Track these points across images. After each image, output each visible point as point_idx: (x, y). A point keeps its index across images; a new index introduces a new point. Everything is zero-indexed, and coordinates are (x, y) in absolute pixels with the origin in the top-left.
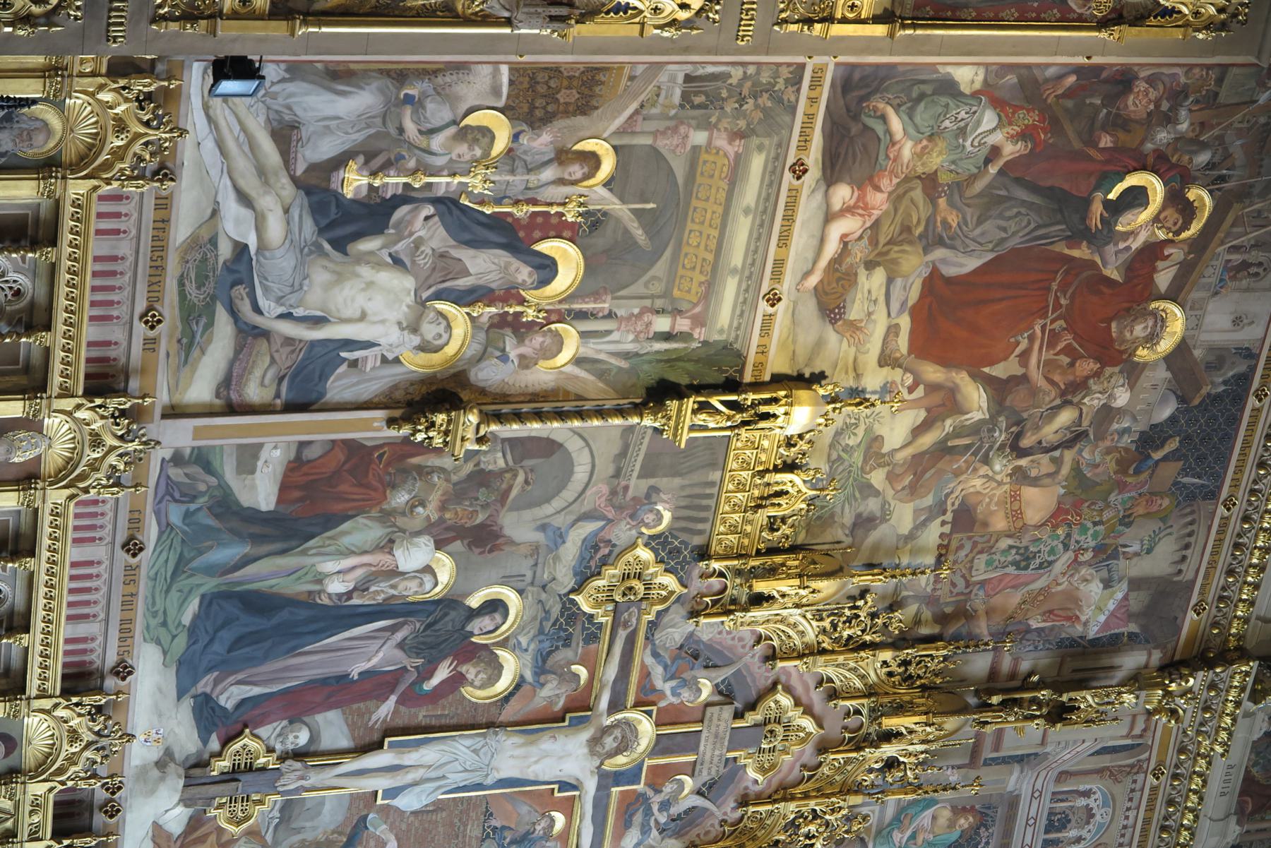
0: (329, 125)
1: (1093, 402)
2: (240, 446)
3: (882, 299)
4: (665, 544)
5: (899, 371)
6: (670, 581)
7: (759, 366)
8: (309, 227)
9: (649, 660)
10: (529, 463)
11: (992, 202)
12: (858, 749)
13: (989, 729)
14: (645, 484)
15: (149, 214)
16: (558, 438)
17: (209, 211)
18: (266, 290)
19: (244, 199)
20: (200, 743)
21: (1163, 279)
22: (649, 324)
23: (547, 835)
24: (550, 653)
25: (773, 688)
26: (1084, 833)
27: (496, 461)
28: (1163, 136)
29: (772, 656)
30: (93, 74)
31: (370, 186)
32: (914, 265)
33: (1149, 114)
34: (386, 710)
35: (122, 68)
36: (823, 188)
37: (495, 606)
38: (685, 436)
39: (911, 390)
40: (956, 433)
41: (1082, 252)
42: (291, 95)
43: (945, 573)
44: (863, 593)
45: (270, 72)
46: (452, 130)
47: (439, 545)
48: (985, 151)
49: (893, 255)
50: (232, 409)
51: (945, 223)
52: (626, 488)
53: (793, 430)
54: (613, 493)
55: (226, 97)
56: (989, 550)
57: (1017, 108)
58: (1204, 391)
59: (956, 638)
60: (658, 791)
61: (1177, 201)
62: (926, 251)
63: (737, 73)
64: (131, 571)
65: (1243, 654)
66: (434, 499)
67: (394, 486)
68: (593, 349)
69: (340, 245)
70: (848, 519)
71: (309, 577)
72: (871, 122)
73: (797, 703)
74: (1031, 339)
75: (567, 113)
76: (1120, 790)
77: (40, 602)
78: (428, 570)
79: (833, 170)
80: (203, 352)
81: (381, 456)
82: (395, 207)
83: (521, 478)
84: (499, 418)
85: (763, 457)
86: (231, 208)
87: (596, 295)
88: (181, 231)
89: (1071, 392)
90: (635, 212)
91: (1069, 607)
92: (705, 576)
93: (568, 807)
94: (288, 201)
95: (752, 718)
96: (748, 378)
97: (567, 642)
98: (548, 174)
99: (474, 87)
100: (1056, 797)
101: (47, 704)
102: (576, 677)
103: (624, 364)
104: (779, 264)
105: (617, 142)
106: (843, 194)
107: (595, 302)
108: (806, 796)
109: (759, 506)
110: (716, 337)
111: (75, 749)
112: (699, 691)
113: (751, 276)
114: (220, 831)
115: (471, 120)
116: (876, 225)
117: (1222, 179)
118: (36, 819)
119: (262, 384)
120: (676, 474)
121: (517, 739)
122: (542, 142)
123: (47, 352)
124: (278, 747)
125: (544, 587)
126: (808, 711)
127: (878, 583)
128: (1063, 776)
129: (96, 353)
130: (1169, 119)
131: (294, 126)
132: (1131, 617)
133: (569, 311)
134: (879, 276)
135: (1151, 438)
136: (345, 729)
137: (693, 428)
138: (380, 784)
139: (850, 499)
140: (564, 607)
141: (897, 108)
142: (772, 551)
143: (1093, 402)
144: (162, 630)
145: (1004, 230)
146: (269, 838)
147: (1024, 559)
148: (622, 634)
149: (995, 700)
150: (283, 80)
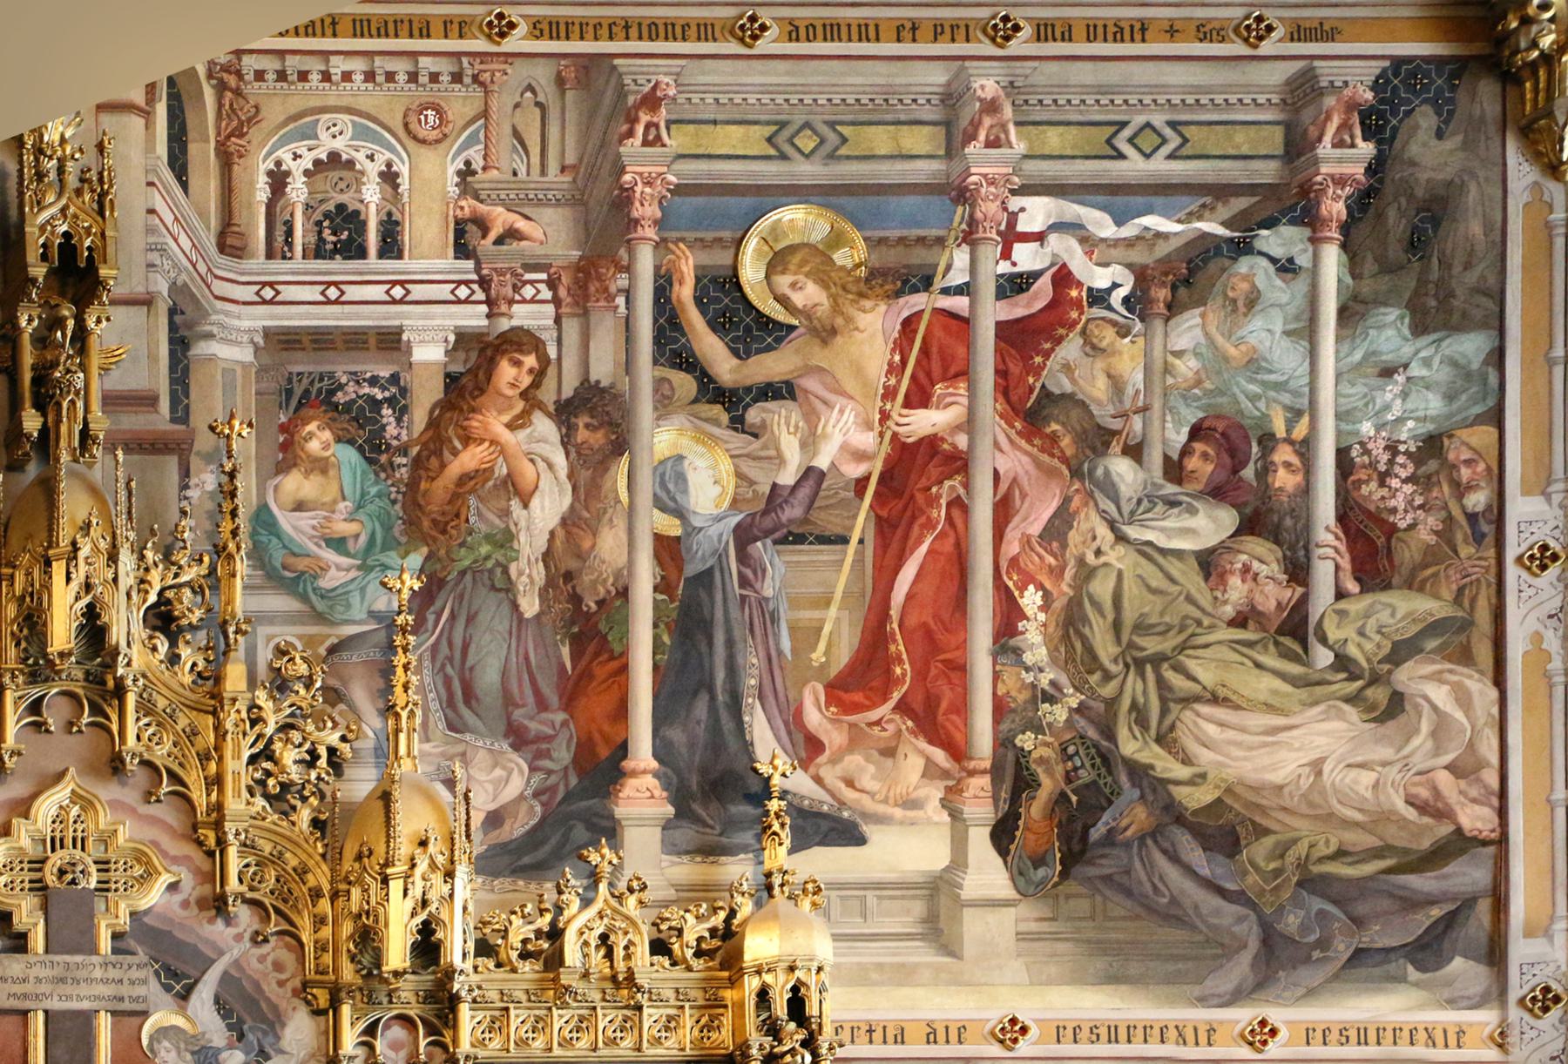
13: (100, 423)
26: (373, 170)
128: (230, 242)
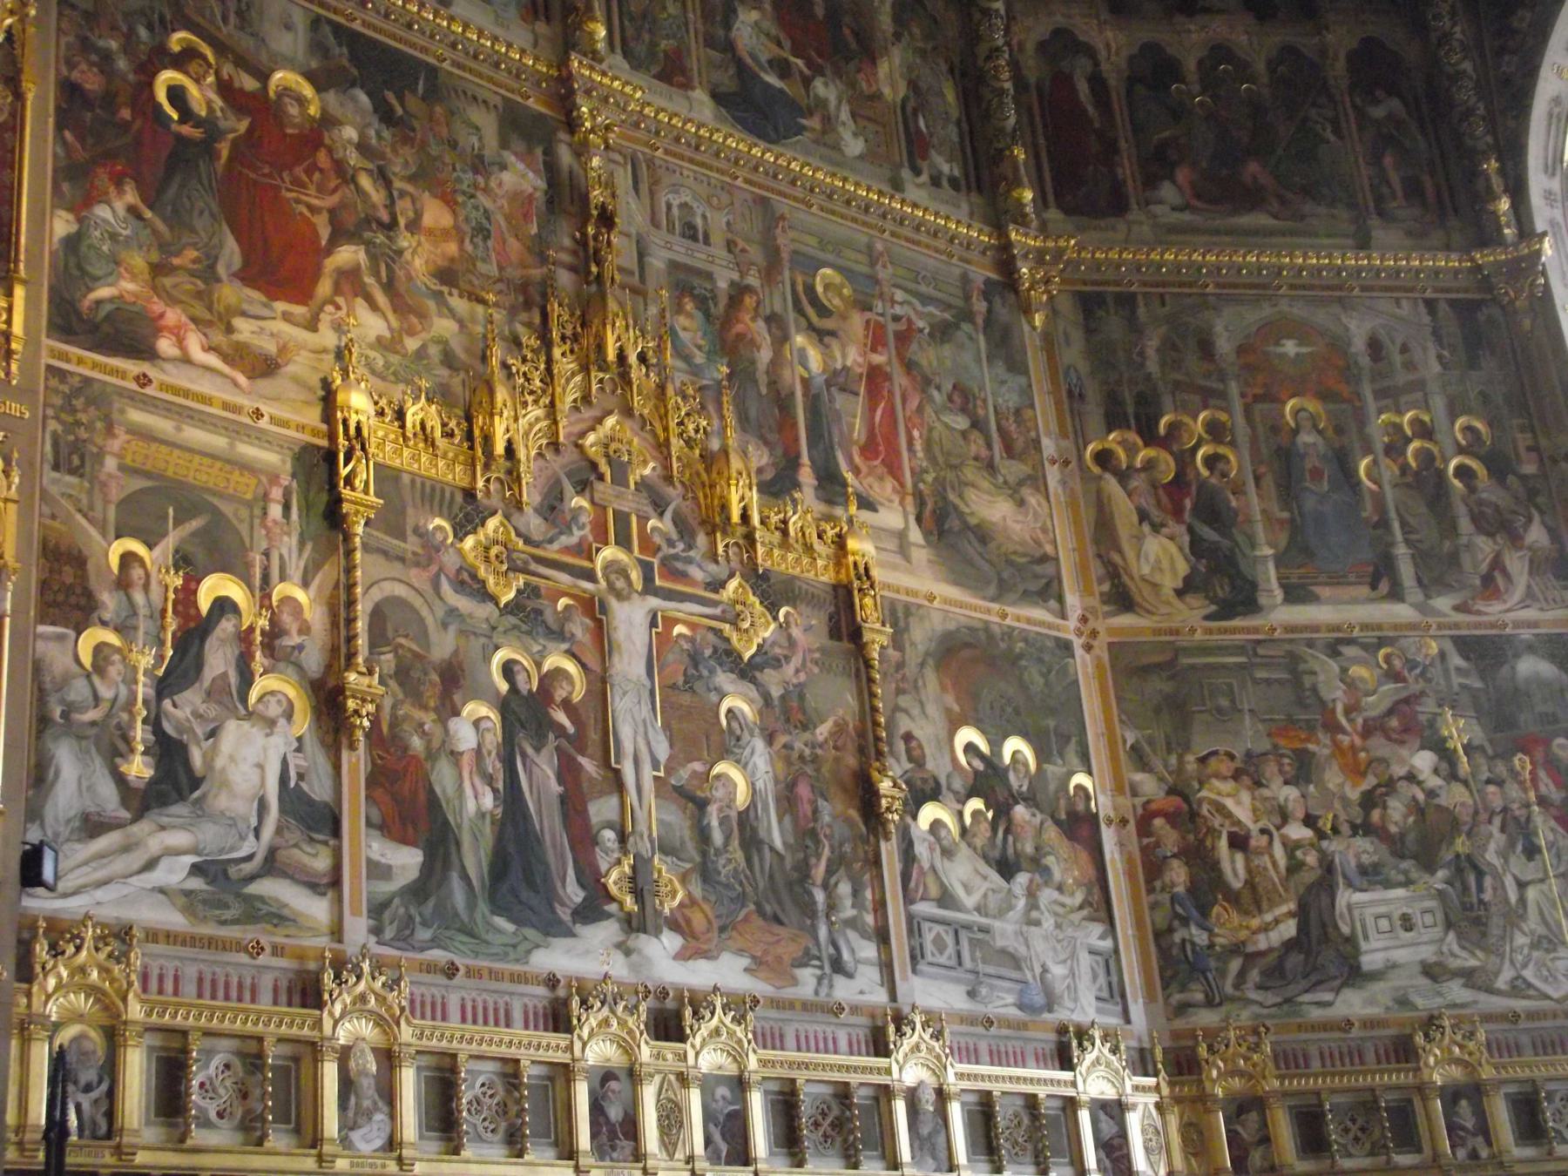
0: (85, 787)
1: (353, 158)
2: (368, 877)
3: (261, 323)
4: (462, 526)
5: (322, 316)
6: (492, 523)
7: (315, 432)
8: (179, 809)
9: (556, 546)
10: (390, 634)
11: (178, 219)
12: (629, 383)
13: (617, 277)
14: (412, 538)
15: (160, 948)
16: (369, 609)
17: (161, 896)
18: (232, 849)
19: (150, 865)
20: (612, 920)
21: (249, 83)
22: (275, 522)
23: (691, 640)
24: (548, 628)
25: (577, 446)
27: (388, 660)
28: (122, 64)
29: (555, 445)
30: (29, 995)
31: (144, 753)
32: (230, 292)
33: (102, 72)
34: (589, 765)
35: (25, 972)
36: (161, 363)
37: (508, 669)
38: (372, 498)
39: (338, 308)
40: (377, 275)
41: (224, 149)
42: (56, 819)
43: (491, 297)
44: (505, 366)
45: (34, 836)
46: (96, 679)
47: (457, 713)
48: (131, 219)
49: (222, 309)
50: (336, 882)
51: (194, 261)
52: (414, 554)
53: (371, 410)
54: (417, 564)
55: (57, 877)
56: (472, 260)
57: (92, 186)
58: (345, 62)
59: (544, 296)
60: (659, 549)
61: (181, 61)
62: (218, 280)
63: (53, 425)
64: (469, 973)
65: (564, 63)
66: (418, 714)
67: (406, 748)
68: (296, 572)
69: (196, 783)
70: (445, 372)
71: (480, 823)
72: (102, 313)
73: (593, 429)
74: (298, 201)
75: (84, 577)
76: (667, 180)
77: (494, 1050)
78: (476, 723)
79: (145, 352)
80: (286, 906)
81: (381, 757)
82: (164, 733)
83: (402, 641)
84: (351, 656)
85: (392, 436)
86: (159, 876)
87: (249, 566)
88: (174, 919)
89: (345, 175)
90: (176, 525)
91: (521, 201)
92: (488, 492)
93: (670, 622)
94: (153, 827)
95: (604, 468)
96: (324, 443)
97: (539, 612)
98: (139, 597)
99: (57, 658)
100: (671, 229)
101: (577, 1046)
102: (567, 607)
103: (309, 546)
104: (226, 406)
105: (112, 534)
106: (165, 345)
107: (253, 566)
108: (666, 429)
109: (433, 445)
110: (288, 466)
111: (614, 1022)
112: (581, 508)
113: (237, 431)
114: (681, 905)
115: (87, 660)
116: (194, 320)
117: (162, 20)
118: (670, 1056)
119: (315, 856)
120: (403, 512)
121: (616, 659)
122: (109, 601)
123: (281, 1040)
124: (616, 855)
125: (494, 628)
126: (600, 420)
127: (497, 353)
128: (655, 223)
129: (283, 998)
130: (107, 57)
131: (86, 818)
132: (530, 151)
133: (262, 589)
134: (238, 322)
135: (386, 115)
136: (602, 800)
137: (366, 491)
138: (648, 773)
139: (428, 369)
140: (511, 613)
141: (90, 290)
142: (469, 436)
143: (353, 158)
144: (521, 948)
145: (201, 213)
146: (688, 866)
147: (482, 232)
148: (533, 566)
149: (594, 269)
150: (42, 826)
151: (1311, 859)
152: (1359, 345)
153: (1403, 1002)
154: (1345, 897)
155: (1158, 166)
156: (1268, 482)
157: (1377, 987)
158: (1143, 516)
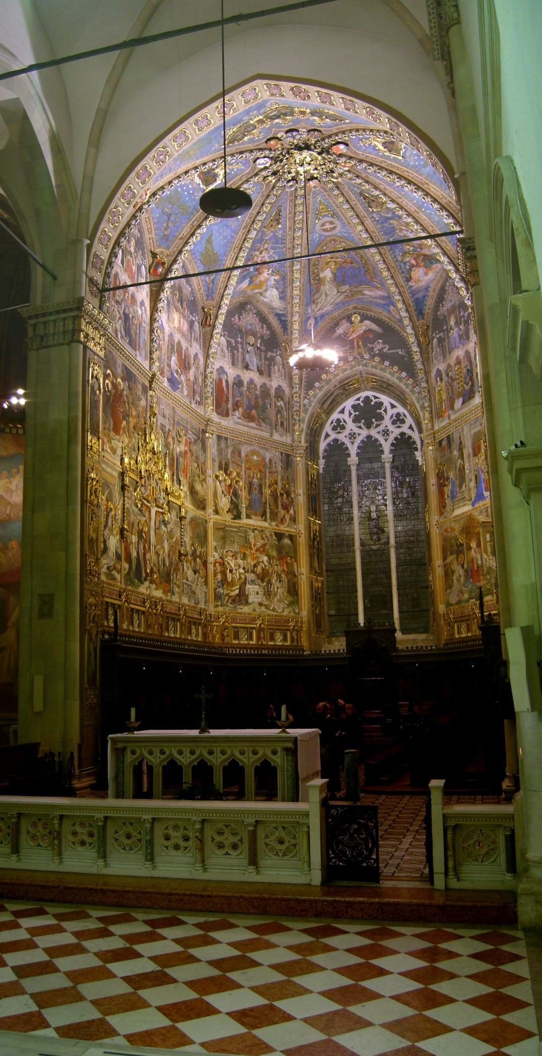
151: (243, 577)
152: (267, 460)
153: (254, 610)
154: (248, 586)
155: (236, 406)
156: (247, 489)
157: (251, 606)
158: (223, 492)
